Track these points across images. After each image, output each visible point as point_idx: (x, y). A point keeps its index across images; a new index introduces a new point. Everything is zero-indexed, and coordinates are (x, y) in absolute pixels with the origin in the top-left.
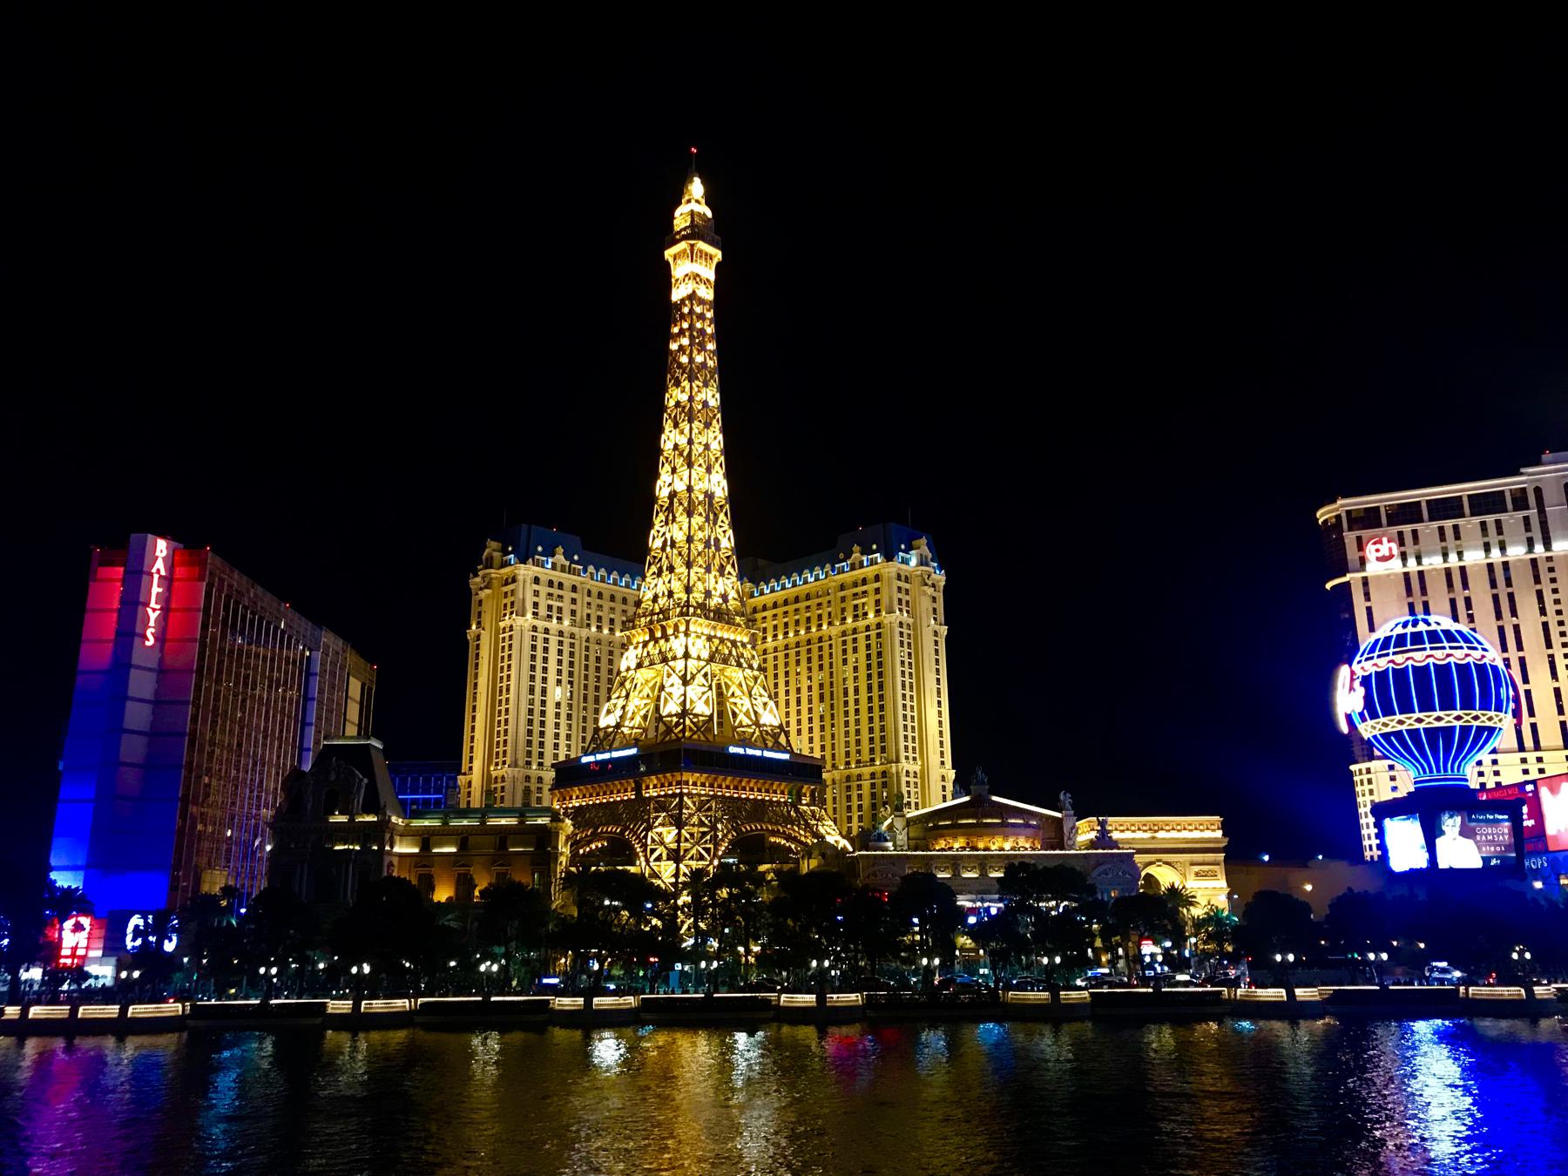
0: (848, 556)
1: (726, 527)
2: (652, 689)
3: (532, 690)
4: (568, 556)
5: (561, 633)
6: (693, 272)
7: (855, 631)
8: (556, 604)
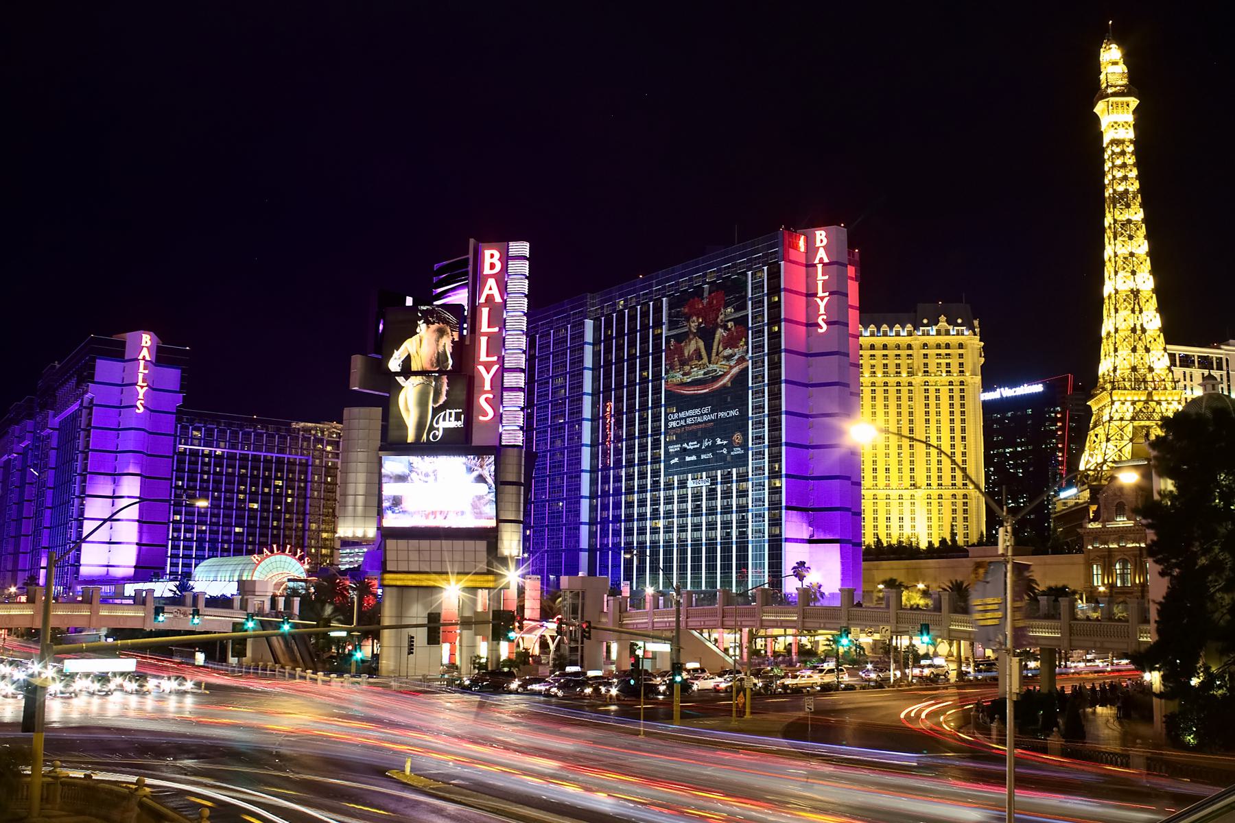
6: (1117, 121)
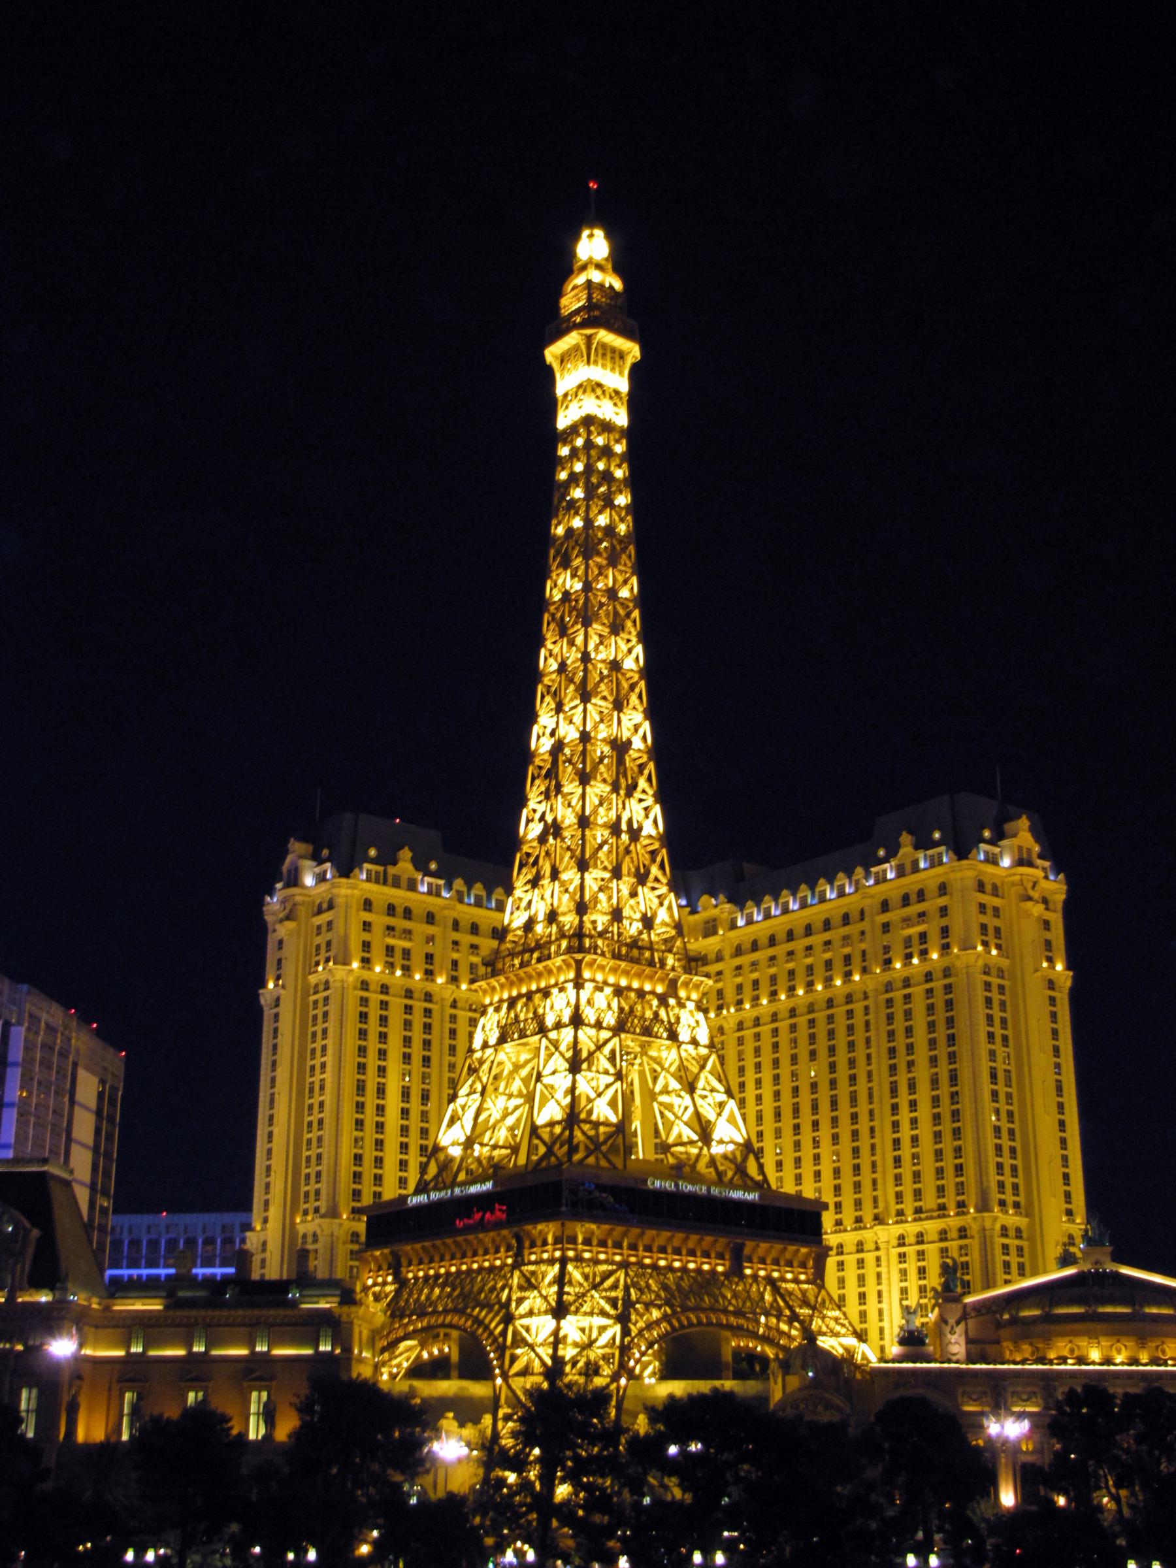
0: (892, 853)
1: (650, 801)
2: (526, 1081)
3: (361, 1088)
4: (420, 865)
5: (409, 994)
6: (591, 384)
7: (907, 982)
8: (400, 944)
